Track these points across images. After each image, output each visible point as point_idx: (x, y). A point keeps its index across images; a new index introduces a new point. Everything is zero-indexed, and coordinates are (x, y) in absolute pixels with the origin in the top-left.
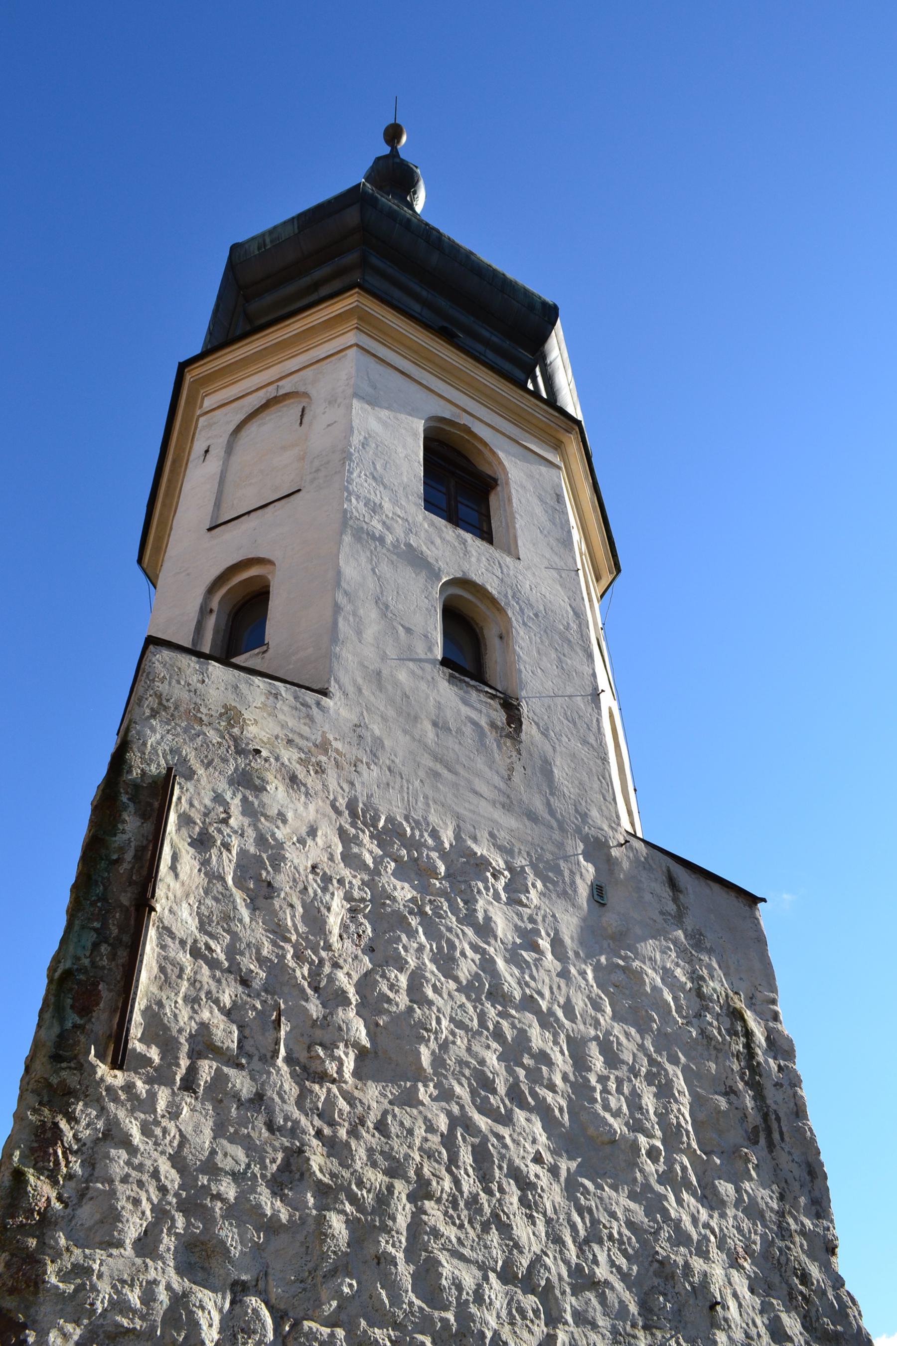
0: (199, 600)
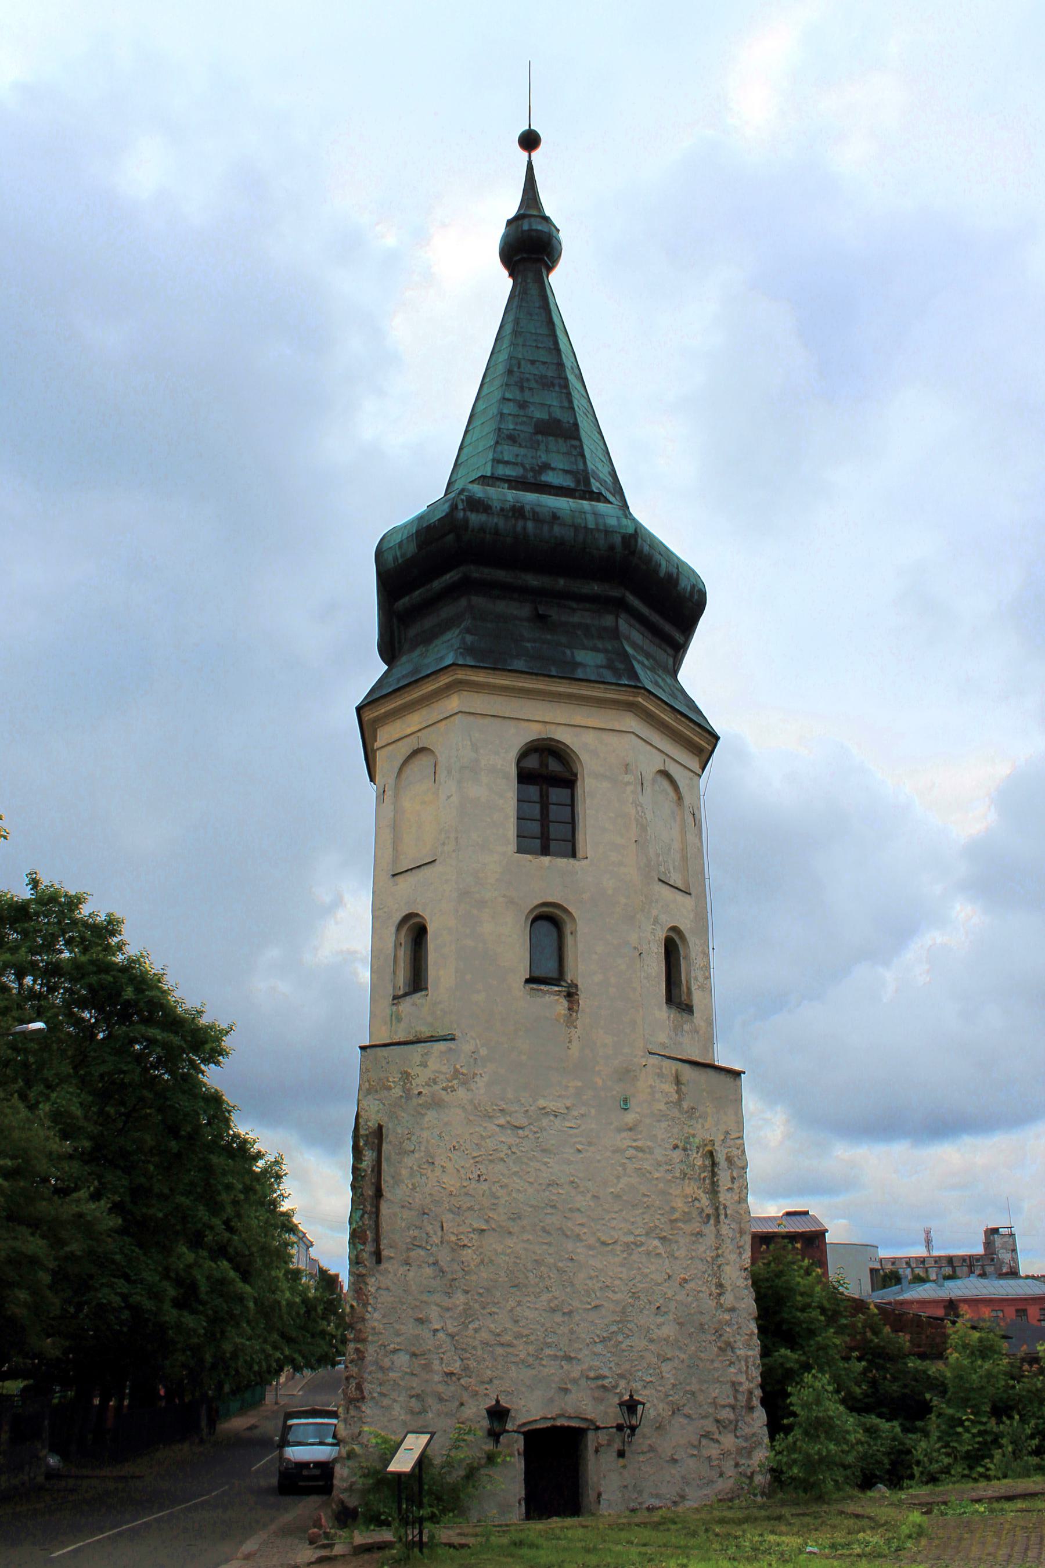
0: (393, 938)
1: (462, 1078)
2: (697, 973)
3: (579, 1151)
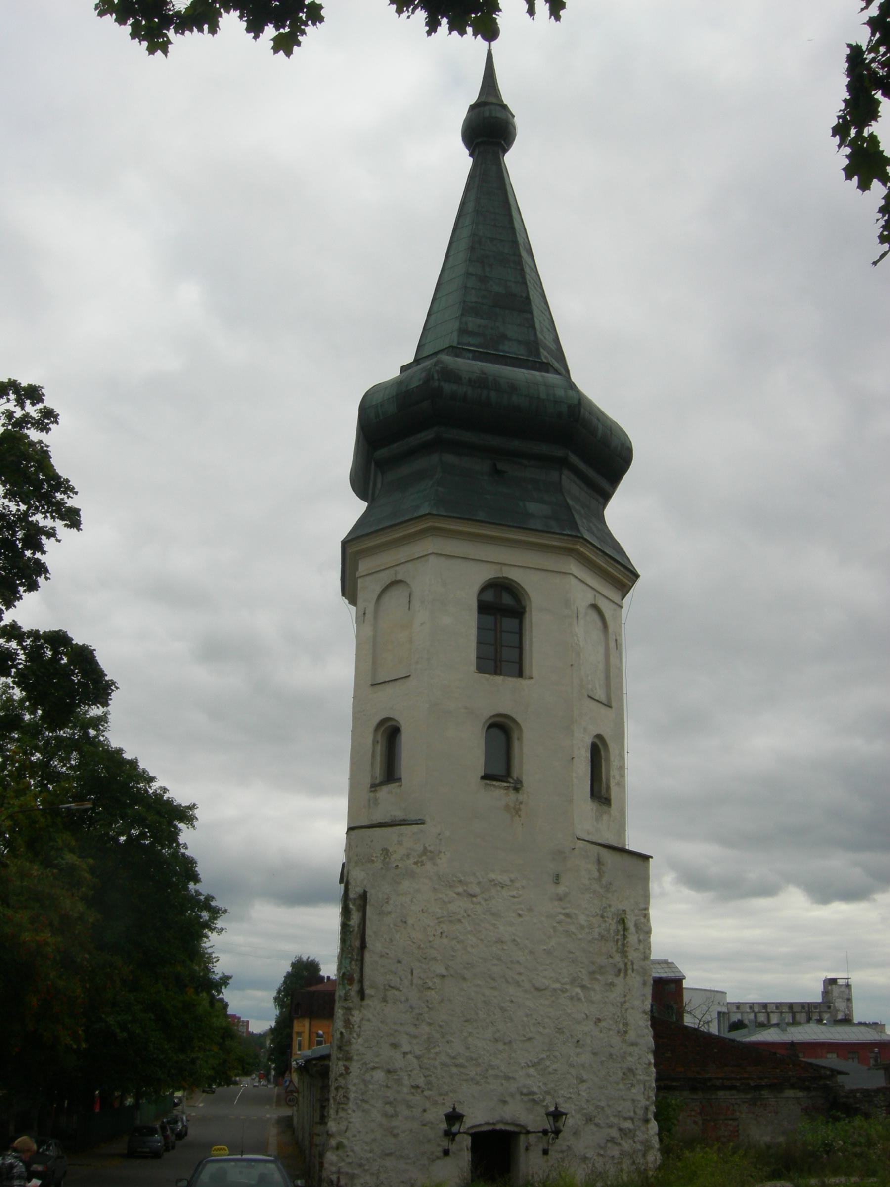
1: (428, 854)
2: (614, 772)
3: (520, 915)
